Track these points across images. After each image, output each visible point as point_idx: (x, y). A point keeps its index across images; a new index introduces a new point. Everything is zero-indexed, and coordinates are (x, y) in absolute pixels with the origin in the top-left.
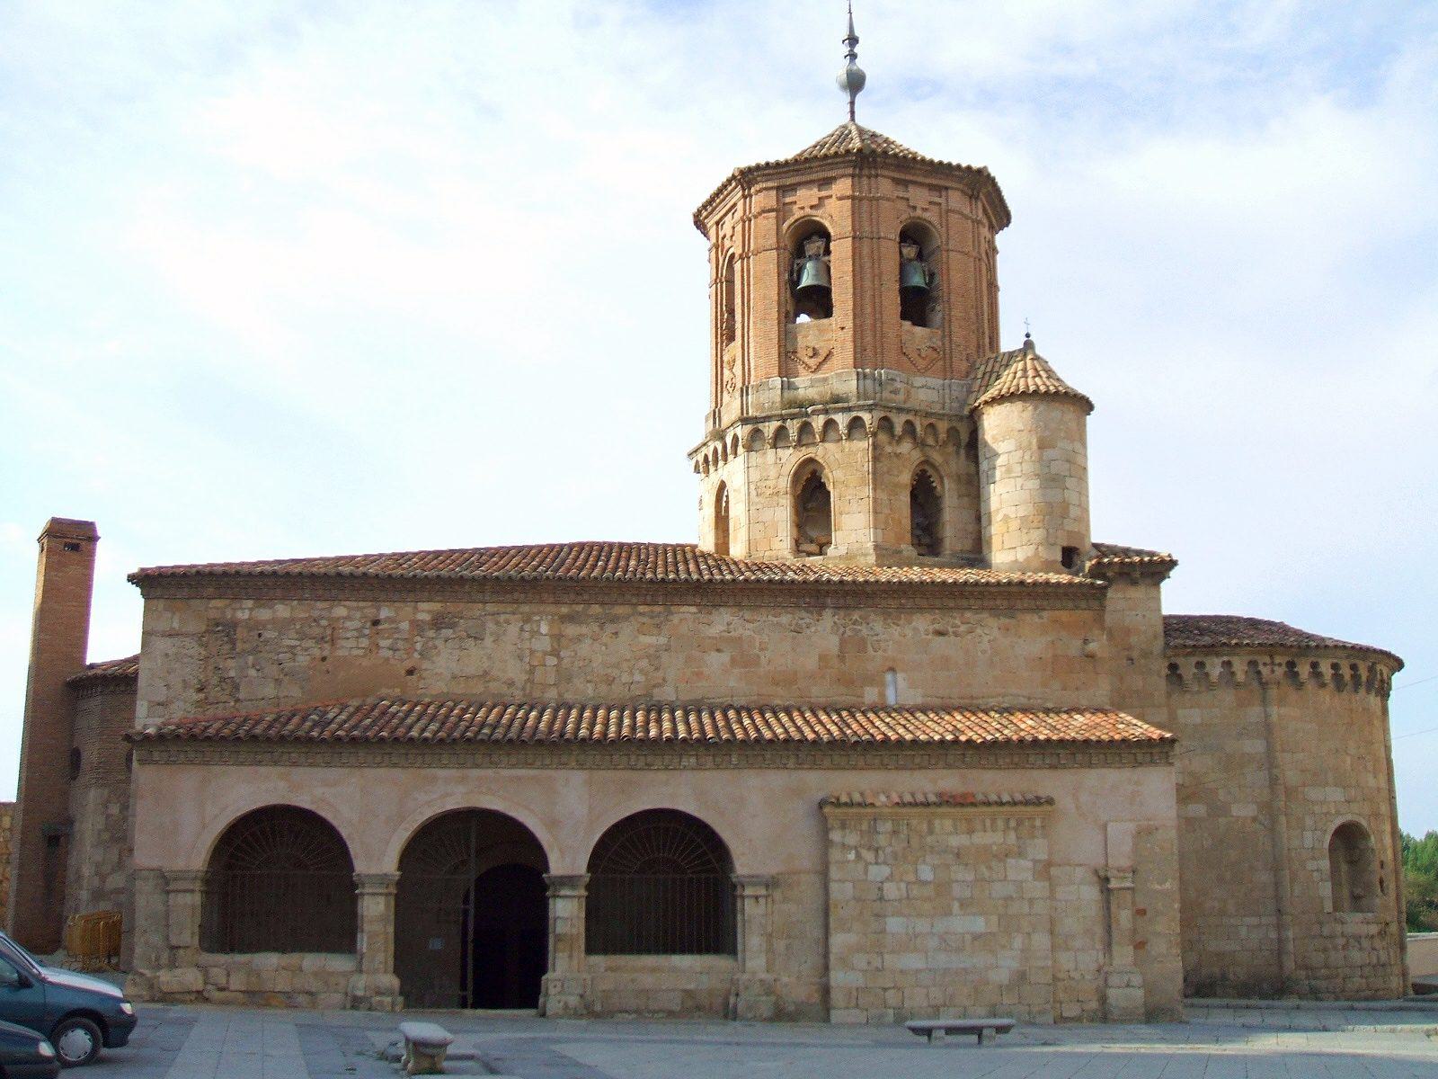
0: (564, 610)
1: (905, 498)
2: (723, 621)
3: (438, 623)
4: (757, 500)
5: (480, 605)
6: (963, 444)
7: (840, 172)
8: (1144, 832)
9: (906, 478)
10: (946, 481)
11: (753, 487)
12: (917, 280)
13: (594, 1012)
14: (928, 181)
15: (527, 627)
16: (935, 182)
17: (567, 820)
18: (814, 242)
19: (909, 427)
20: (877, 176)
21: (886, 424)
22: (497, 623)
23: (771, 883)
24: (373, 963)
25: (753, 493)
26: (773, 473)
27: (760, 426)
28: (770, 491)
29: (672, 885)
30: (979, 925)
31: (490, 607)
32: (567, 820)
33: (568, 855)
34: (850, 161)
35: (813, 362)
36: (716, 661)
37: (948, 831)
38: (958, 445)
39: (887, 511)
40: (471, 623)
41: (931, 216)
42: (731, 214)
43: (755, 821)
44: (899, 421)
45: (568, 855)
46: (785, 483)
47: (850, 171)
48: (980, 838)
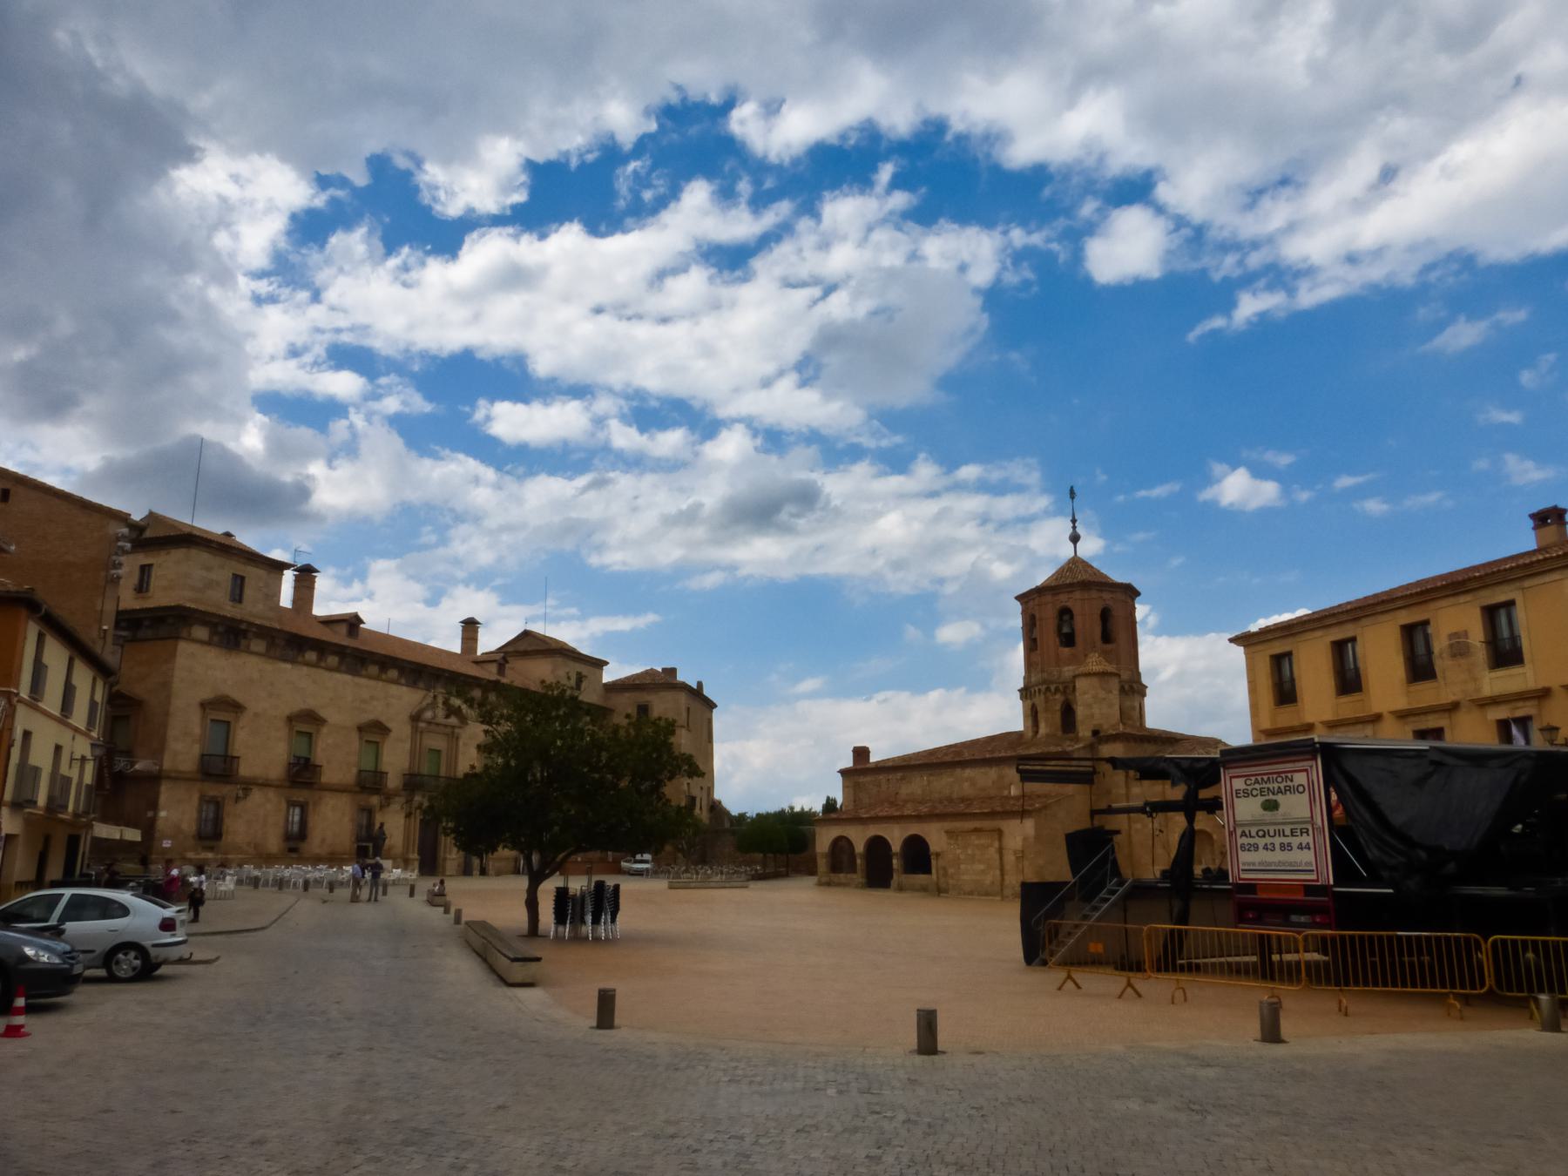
1: (1058, 716)
2: (968, 772)
3: (903, 779)
8: (1025, 839)
9: (1058, 707)
12: (1066, 630)
13: (901, 889)
17: (896, 837)
19: (1057, 690)
21: (1048, 689)
23: (938, 855)
24: (858, 877)
29: (918, 856)
30: (982, 867)
32: (896, 837)
33: (896, 847)
36: (966, 784)
37: (975, 840)
41: (1069, 604)
43: (935, 836)
44: (1053, 688)
45: (896, 847)
48: (983, 841)
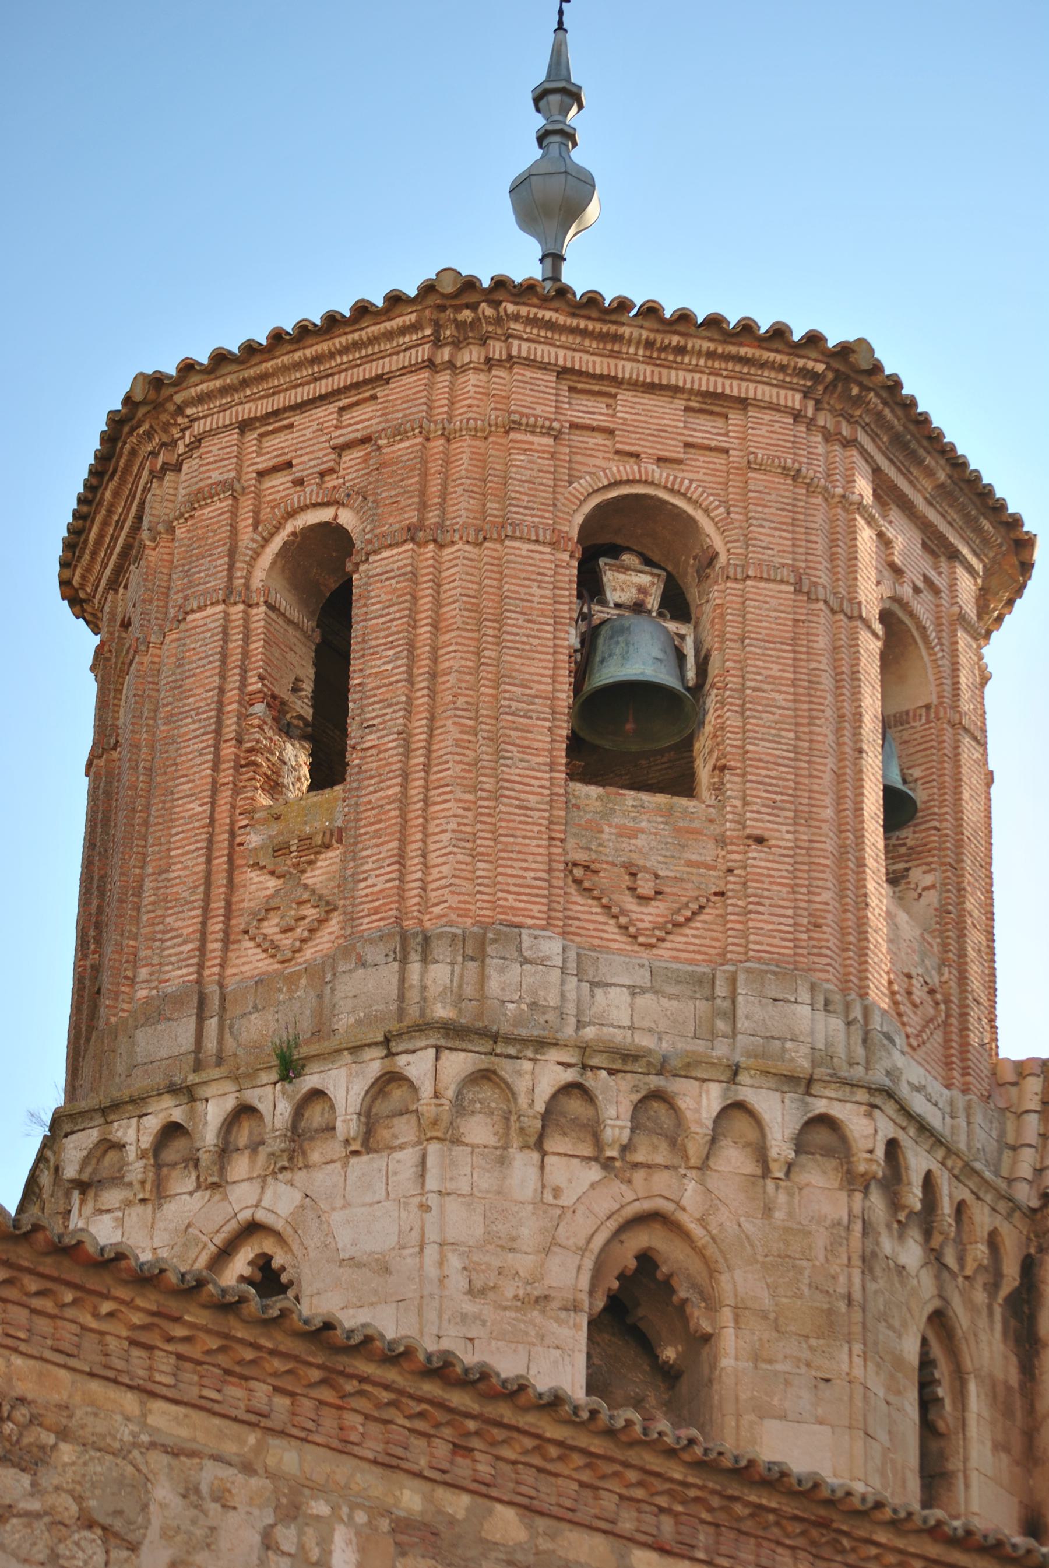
0: (411, 1499)
4: (469, 1307)
5: (130, 1401)
6: (1005, 1290)
7: (765, 393)
10: (972, 1387)
11: (455, 1262)
14: (932, 516)
15: (287, 1537)
16: (943, 527)
18: (626, 569)
20: (848, 443)
22: (190, 1492)
25: (458, 1282)
26: (529, 1232)
27: (506, 1069)
28: (510, 1289)
31: (164, 1418)
34: (805, 373)
35: (647, 916)
38: (993, 1288)
39: (883, 1436)
40: (100, 1467)
42: (333, 407)
46: (570, 1275)
47: (795, 400)
